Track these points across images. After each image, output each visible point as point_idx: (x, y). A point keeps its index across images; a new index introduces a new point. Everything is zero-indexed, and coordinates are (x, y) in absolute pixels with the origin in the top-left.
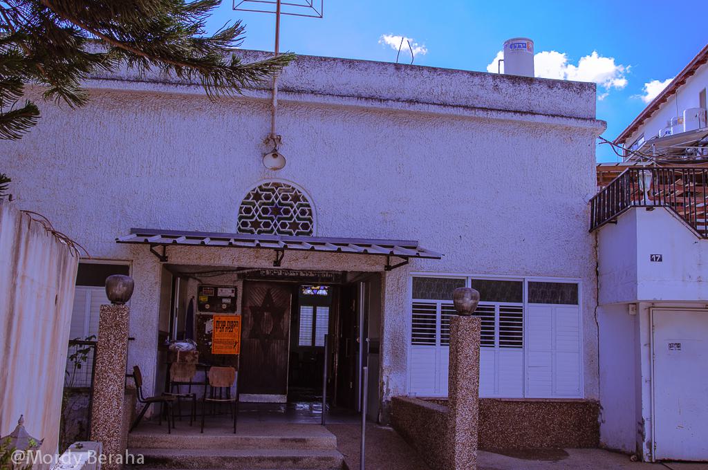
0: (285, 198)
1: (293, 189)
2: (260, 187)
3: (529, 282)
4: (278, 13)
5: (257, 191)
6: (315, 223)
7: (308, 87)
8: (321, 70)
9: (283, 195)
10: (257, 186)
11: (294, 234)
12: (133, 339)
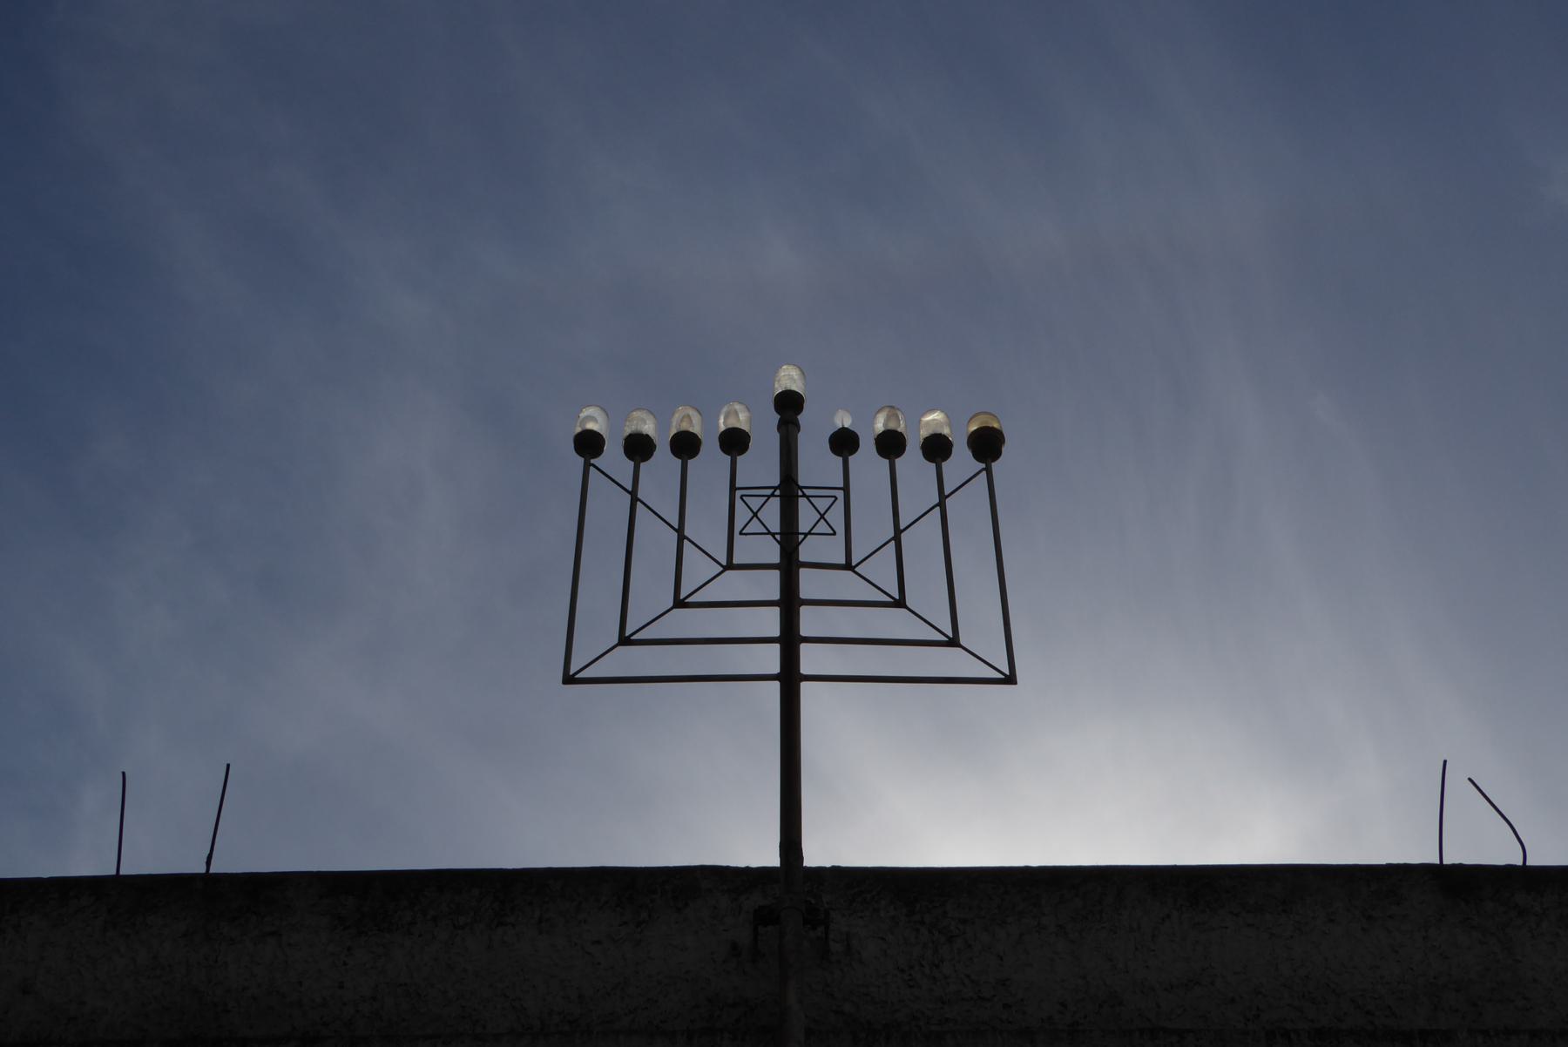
4: (790, 679)
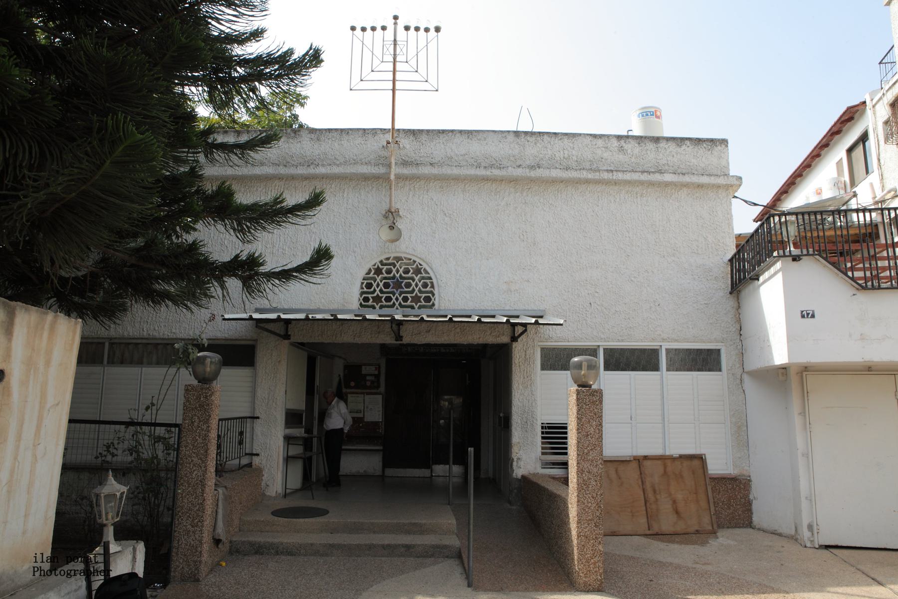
0: (407, 271)
1: (415, 262)
2: (381, 262)
3: (666, 349)
4: (394, 90)
5: (378, 266)
6: (436, 296)
7: (427, 159)
8: (439, 143)
9: (405, 268)
10: (377, 261)
11: (416, 307)
12: (258, 418)
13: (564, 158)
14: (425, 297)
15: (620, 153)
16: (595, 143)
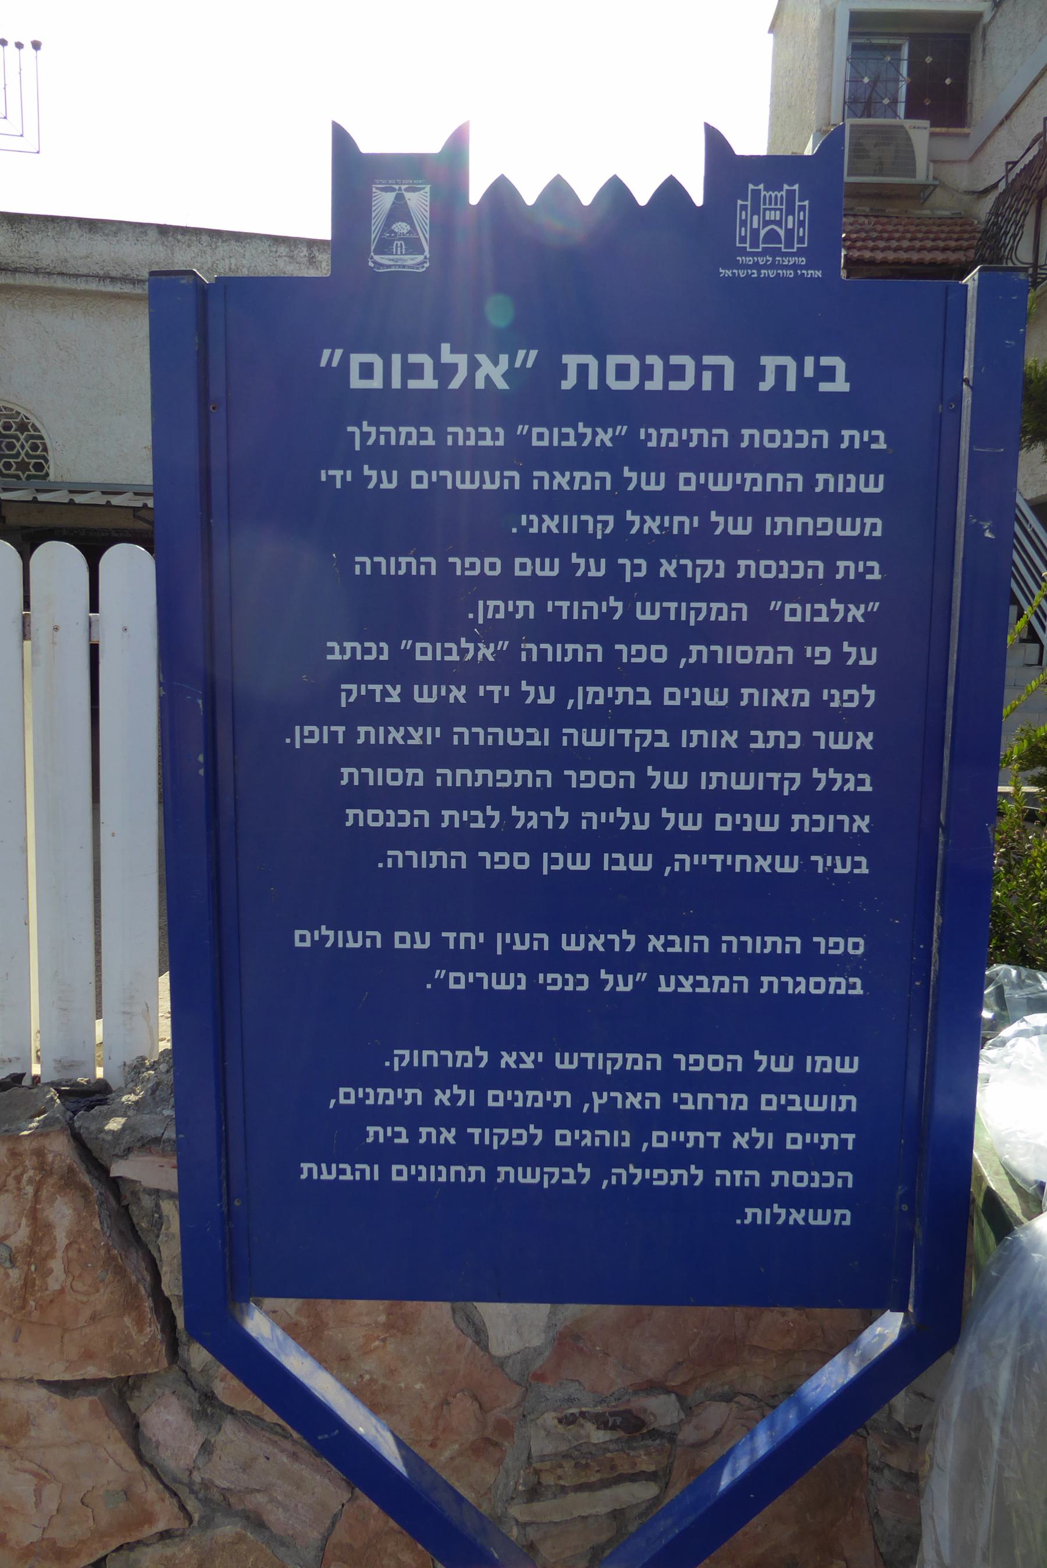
1: (18, 413)
6: (51, 463)
7: (31, 262)
11: (23, 477)
13: (230, 269)
14: (36, 464)
15: (311, 267)
16: (275, 249)
